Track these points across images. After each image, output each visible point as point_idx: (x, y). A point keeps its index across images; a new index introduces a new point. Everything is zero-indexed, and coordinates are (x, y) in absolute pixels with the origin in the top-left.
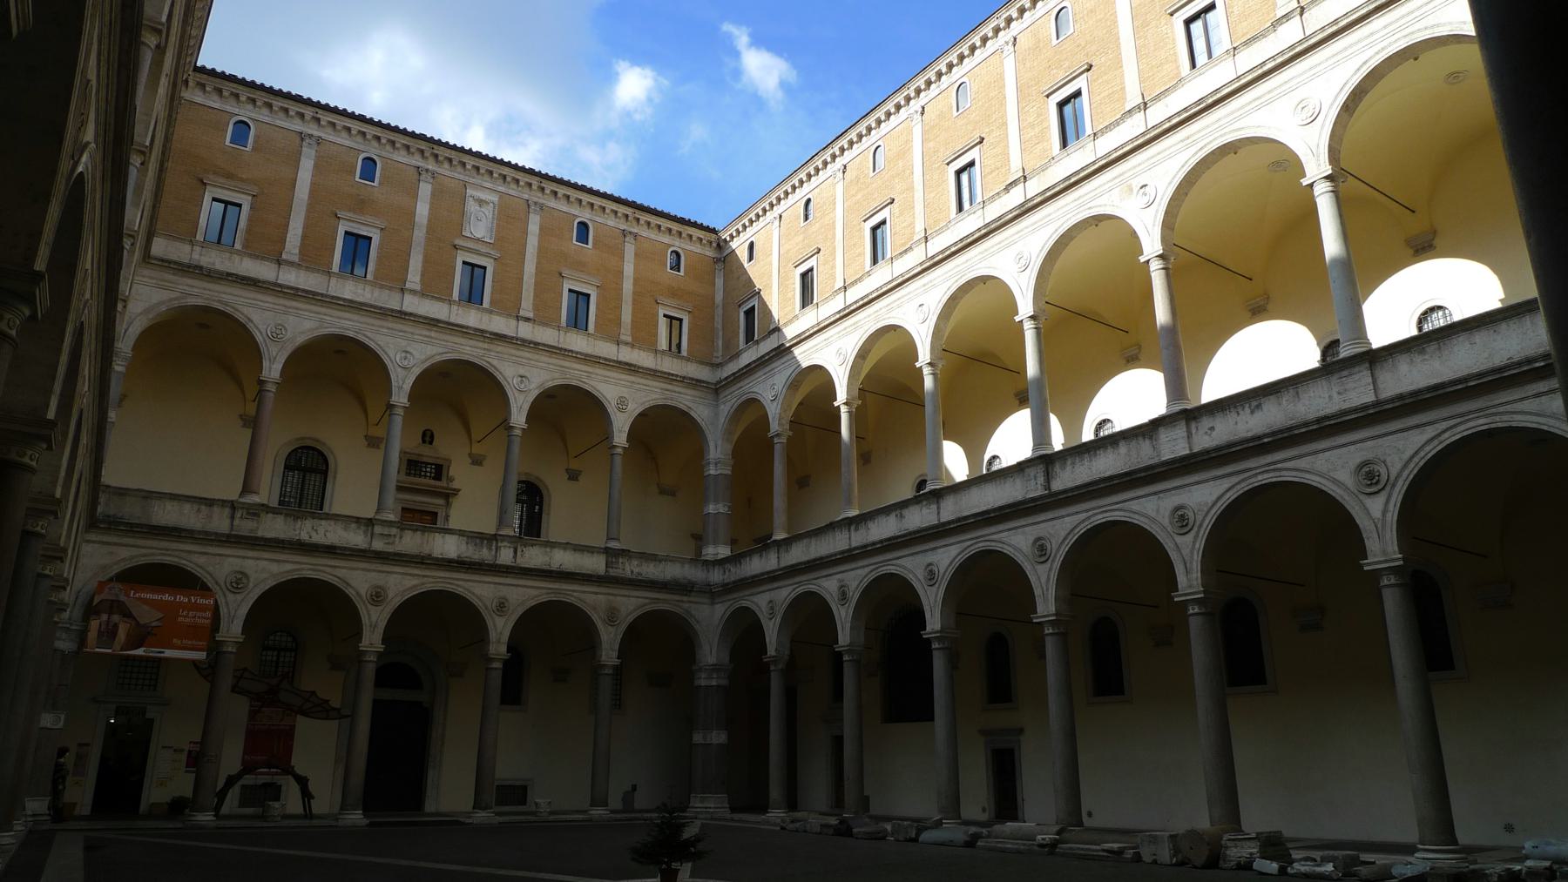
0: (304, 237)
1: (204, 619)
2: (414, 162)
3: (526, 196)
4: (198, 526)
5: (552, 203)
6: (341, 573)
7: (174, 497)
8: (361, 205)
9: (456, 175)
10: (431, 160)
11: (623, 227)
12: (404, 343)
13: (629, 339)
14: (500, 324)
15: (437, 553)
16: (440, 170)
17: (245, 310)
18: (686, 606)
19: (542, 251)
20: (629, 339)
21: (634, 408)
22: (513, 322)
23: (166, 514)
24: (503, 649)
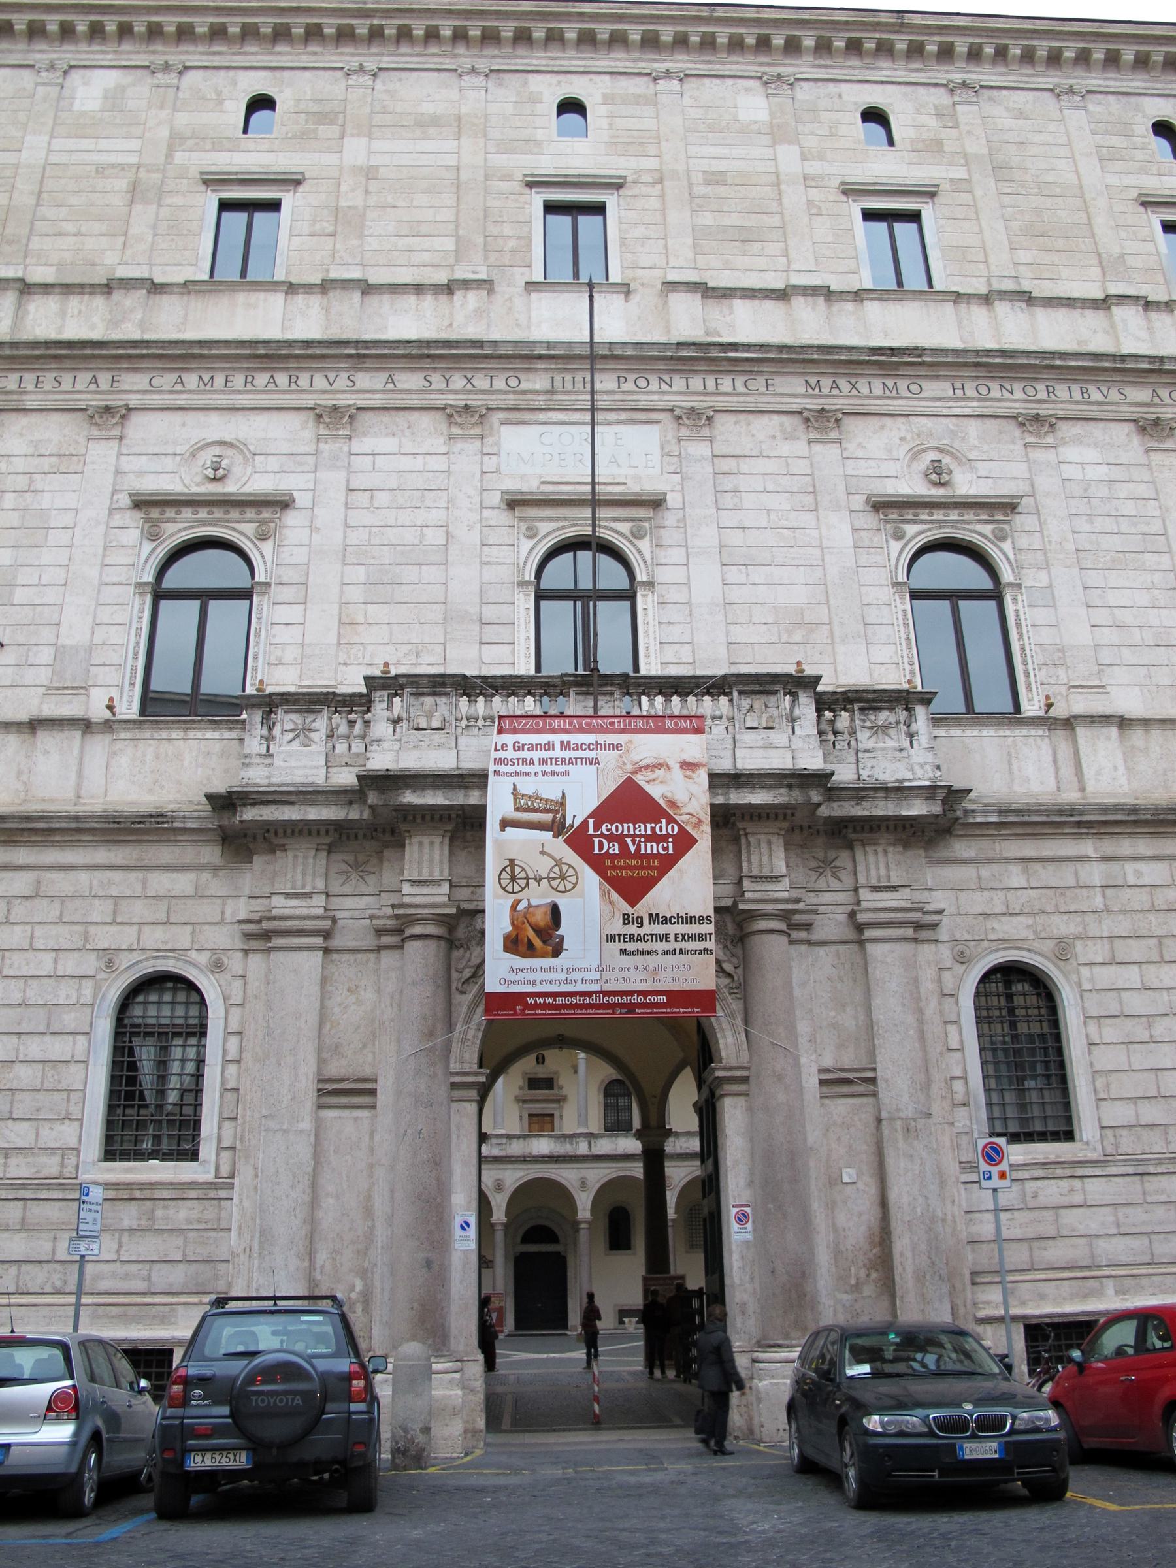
15: (535, 1153)
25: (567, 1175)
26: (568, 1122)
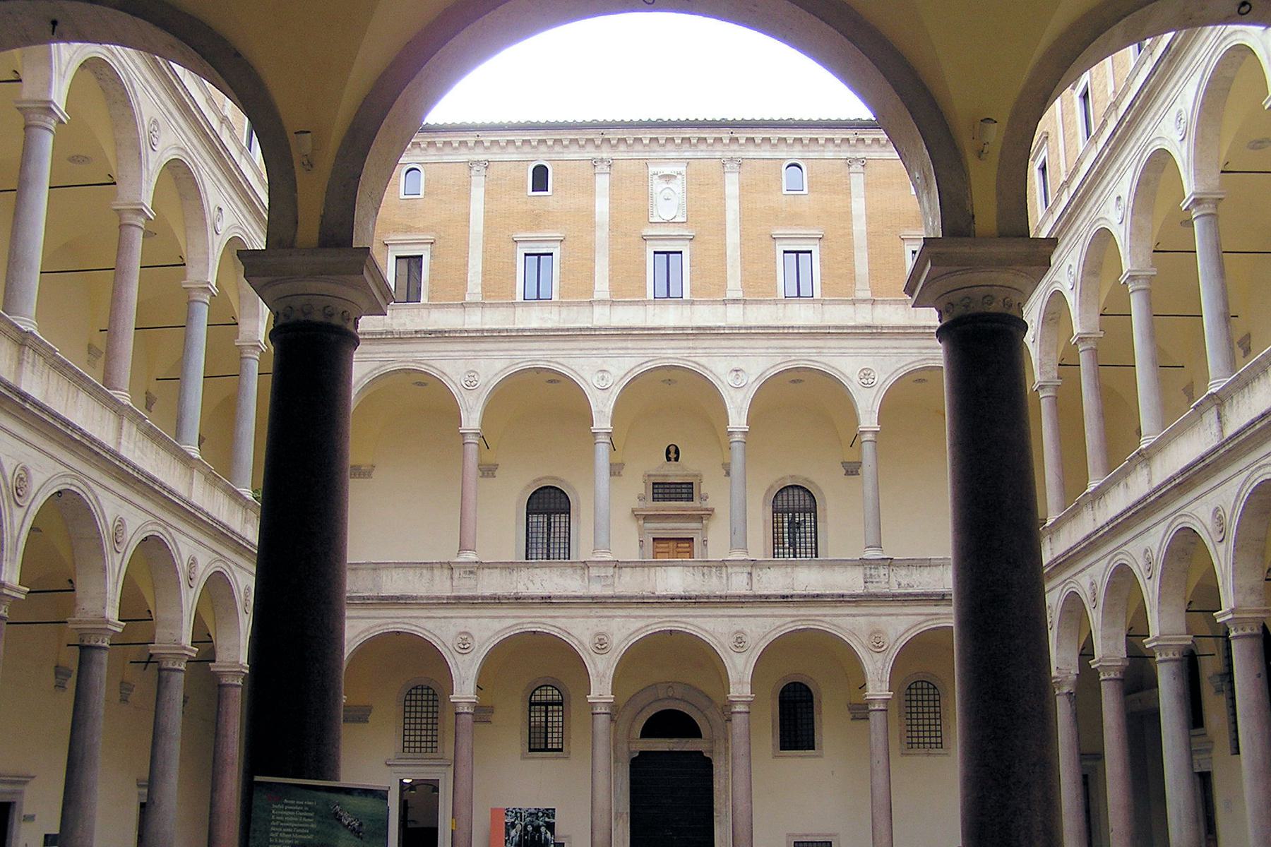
0: (484, 273)
3: (718, 155)
5: (752, 153)
6: (561, 623)
9: (635, 155)
11: (844, 155)
12: (600, 361)
14: (705, 316)
15: (660, 591)
16: (615, 156)
17: (437, 364)
19: (745, 216)
20: (868, 295)
24: (747, 690)
25: (711, 628)
26: (717, 541)
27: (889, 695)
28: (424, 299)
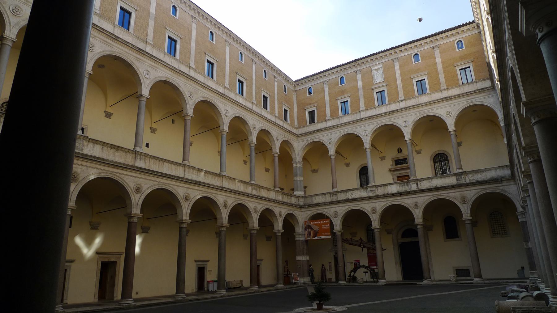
1: (328, 226)
2: (354, 70)
3: (391, 58)
4: (324, 201)
5: (402, 55)
6: (361, 206)
7: (317, 195)
8: (342, 92)
10: (358, 66)
11: (431, 46)
13: (446, 87)
14: (394, 107)
15: (390, 192)
17: (321, 138)
18: (501, 188)
20: (446, 87)
21: (455, 113)
22: (398, 104)
23: (316, 200)
27: (471, 218)
28: (316, 122)
